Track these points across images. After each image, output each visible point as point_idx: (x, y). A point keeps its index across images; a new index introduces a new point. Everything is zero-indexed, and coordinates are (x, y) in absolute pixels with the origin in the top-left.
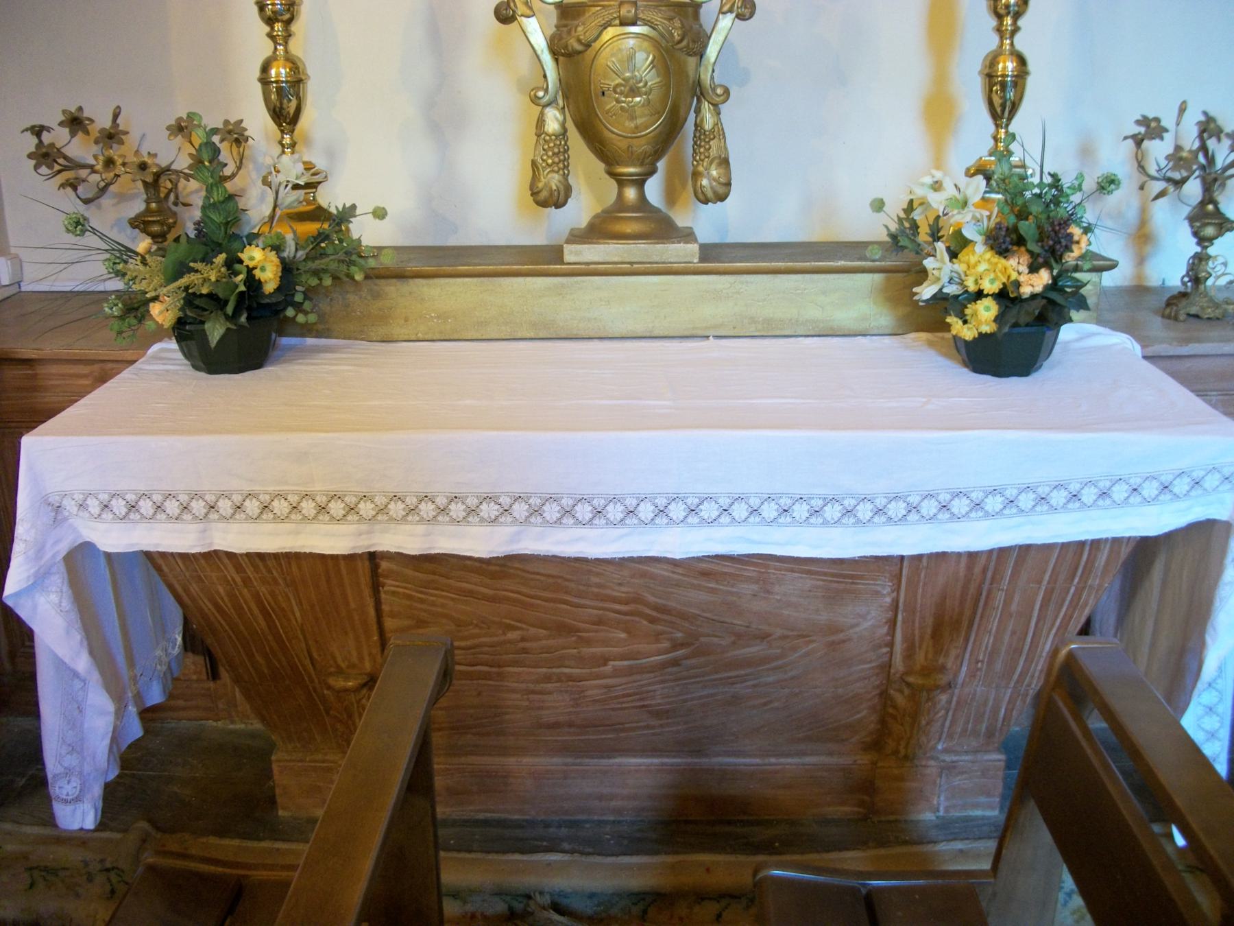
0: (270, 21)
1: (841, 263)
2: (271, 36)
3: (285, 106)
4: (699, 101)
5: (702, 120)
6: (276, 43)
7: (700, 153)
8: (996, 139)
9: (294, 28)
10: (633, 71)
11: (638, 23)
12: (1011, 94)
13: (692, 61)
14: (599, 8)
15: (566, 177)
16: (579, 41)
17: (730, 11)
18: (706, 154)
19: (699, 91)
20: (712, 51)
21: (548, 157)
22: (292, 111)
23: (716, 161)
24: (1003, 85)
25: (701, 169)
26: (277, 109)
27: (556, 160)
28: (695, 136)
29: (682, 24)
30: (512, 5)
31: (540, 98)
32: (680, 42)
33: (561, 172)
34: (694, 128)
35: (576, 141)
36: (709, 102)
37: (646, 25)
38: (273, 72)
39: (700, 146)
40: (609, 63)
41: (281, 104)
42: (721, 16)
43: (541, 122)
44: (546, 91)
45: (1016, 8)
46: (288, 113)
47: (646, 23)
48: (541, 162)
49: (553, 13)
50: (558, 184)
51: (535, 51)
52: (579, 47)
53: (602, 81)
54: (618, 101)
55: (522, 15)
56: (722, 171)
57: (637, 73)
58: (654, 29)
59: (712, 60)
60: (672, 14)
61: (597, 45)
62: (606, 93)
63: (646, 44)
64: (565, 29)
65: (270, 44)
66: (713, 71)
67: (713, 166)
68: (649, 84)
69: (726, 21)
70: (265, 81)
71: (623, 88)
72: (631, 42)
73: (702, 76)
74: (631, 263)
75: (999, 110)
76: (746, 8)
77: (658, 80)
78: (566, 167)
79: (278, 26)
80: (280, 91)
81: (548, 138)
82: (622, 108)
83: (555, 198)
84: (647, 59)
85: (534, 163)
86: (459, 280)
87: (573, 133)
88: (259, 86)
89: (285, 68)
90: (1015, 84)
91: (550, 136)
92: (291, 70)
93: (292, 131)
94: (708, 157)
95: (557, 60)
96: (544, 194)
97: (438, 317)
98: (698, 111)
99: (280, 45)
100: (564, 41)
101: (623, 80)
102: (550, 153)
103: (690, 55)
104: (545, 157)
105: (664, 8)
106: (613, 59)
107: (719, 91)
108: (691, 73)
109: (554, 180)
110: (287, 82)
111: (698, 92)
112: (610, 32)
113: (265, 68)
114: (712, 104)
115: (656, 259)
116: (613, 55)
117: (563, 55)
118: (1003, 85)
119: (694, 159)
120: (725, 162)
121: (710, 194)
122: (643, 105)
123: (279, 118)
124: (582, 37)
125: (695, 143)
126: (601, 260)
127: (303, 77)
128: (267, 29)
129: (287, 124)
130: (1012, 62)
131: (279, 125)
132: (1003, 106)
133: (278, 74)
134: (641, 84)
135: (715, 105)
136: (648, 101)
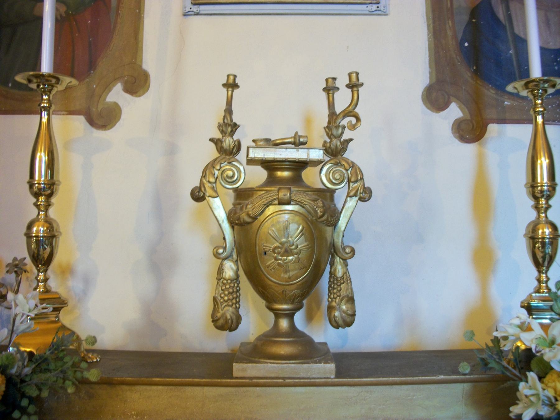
0: (37, 195)
1: (442, 377)
2: (35, 205)
3: (41, 253)
4: (333, 257)
5: (335, 270)
6: (39, 210)
7: (334, 293)
8: (539, 281)
9: (53, 200)
10: (287, 238)
11: (292, 203)
12: (549, 250)
13: (329, 229)
14: (263, 192)
15: (237, 309)
16: (248, 215)
17: (355, 195)
18: (338, 294)
19: (333, 251)
20: (342, 223)
21: (225, 295)
22: (46, 256)
23: (346, 299)
24: (543, 244)
25: (334, 304)
26: (36, 255)
27: (231, 297)
28: (330, 281)
29: (323, 203)
30: (203, 189)
31: (220, 254)
32: (322, 216)
33: (234, 306)
34: (329, 275)
35: (245, 284)
36: (340, 258)
37: (297, 204)
38: (35, 229)
39: (334, 288)
40: (270, 232)
41: (39, 251)
42: (348, 199)
43: (220, 270)
44: (225, 248)
45: (548, 193)
46: (43, 257)
47: (297, 203)
48: (220, 298)
49: (230, 198)
50: (232, 315)
51: (218, 221)
52: (248, 220)
53: (265, 244)
54: (276, 259)
55: (209, 196)
56: (349, 306)
57: (290, 239)
58: (303, 207)
59: (343, 229)
60: (316, 197)
61: (261, 218)
62: (267, 253)
63: (297, 218)
64: (239, 206)
65: (36, 211)
66: (343, 236)
67: (343, 302)
68: (299, 247)
69: (351, 203)
70: (28, 236)
71: (280, 250)
72: (287, 217)
73: (336, 240)
74: (284, 378)
75: (541, 260)
76: (366, 193)
77: (306, 244)
78: (238, 302)
79: (42, 199)
80: (38, 242)
81: (225, 282)
82: (279, 264)
83: (229, 325)
84: (298, 228)
85: (215, 299)
86: (155, 388)
87: (243, 278)
88: (24, 239)
89: (43, 227)
90: (551, 243)
91: (227, 280)
92: (47, 228)
93: (46, 271)
94: (340, 296)
95: (233, 227)
96: (221, 322)
97: (137, 415)
98: (332, 264)
99: (42, 211)
100: (237, 215)
101: (281, 243)
102: (226, 293)
103: (329, 226)
104: (223, 295)
105: (310, 193)
106: (273, 229)
107: (348, 250)
108: (329, 239)
109: (229, 312)
110: (43, 237)
111: (333, 251)
112: (271, 209)
113: (30, 226)
114: (343, 259)
115: (302, 375)
116: (272, 226)
117: (237, 224)
118: (543, 244)
119: (329, 297)
120: (351, 300)
121: (340, 322)
122: (294, 262)
123: (37, 262)
124: (250, 213)
125: (330, 286)
126: (261, 376)
127: (56, 234)
128: (34, 200)
129: (42, 265)
130: (548, 229)
131: (37, 266)
132: (544, 258)
133: (38, 231)
134: (293, 247)
135: (345, 260)
136: (299, 259)
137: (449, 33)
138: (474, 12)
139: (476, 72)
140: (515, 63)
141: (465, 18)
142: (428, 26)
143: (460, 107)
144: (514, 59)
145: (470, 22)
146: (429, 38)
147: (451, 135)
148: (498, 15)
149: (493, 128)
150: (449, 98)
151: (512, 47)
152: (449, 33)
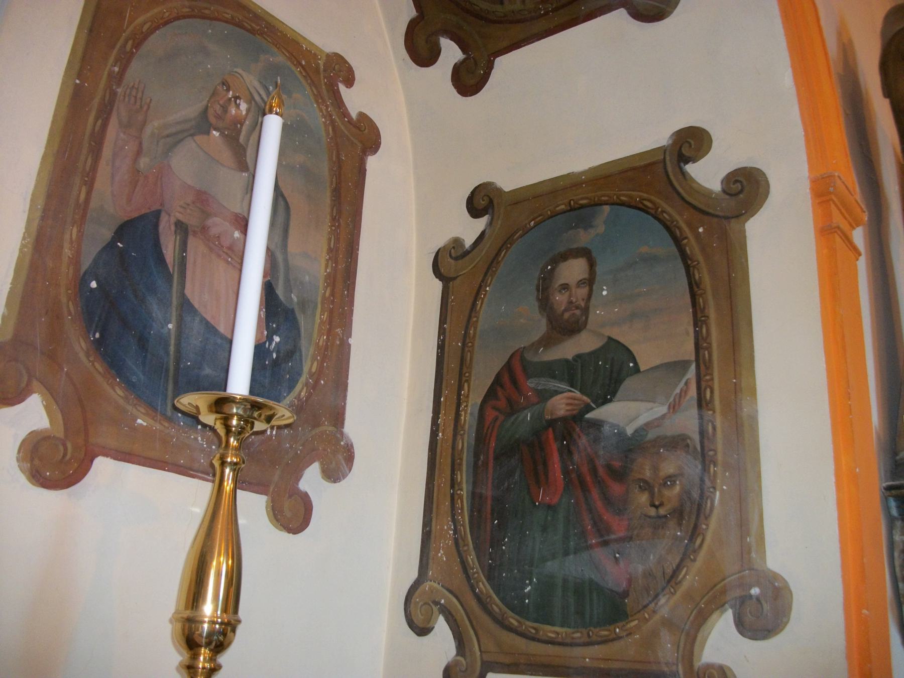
137: (67, 252)
138: (124, 230)
139: (99, 344)
140: (172, 349)
141: (107, 234)
142: (29, 221)
143: (47, 408)
144: (173, 342)
145: (110, 246)
146: (23, 246)
147: (15, 464)
148: (164, 252)
149: (103, 465)
150: (29, 383)
151: (174, 319)
152: (67, 252)
